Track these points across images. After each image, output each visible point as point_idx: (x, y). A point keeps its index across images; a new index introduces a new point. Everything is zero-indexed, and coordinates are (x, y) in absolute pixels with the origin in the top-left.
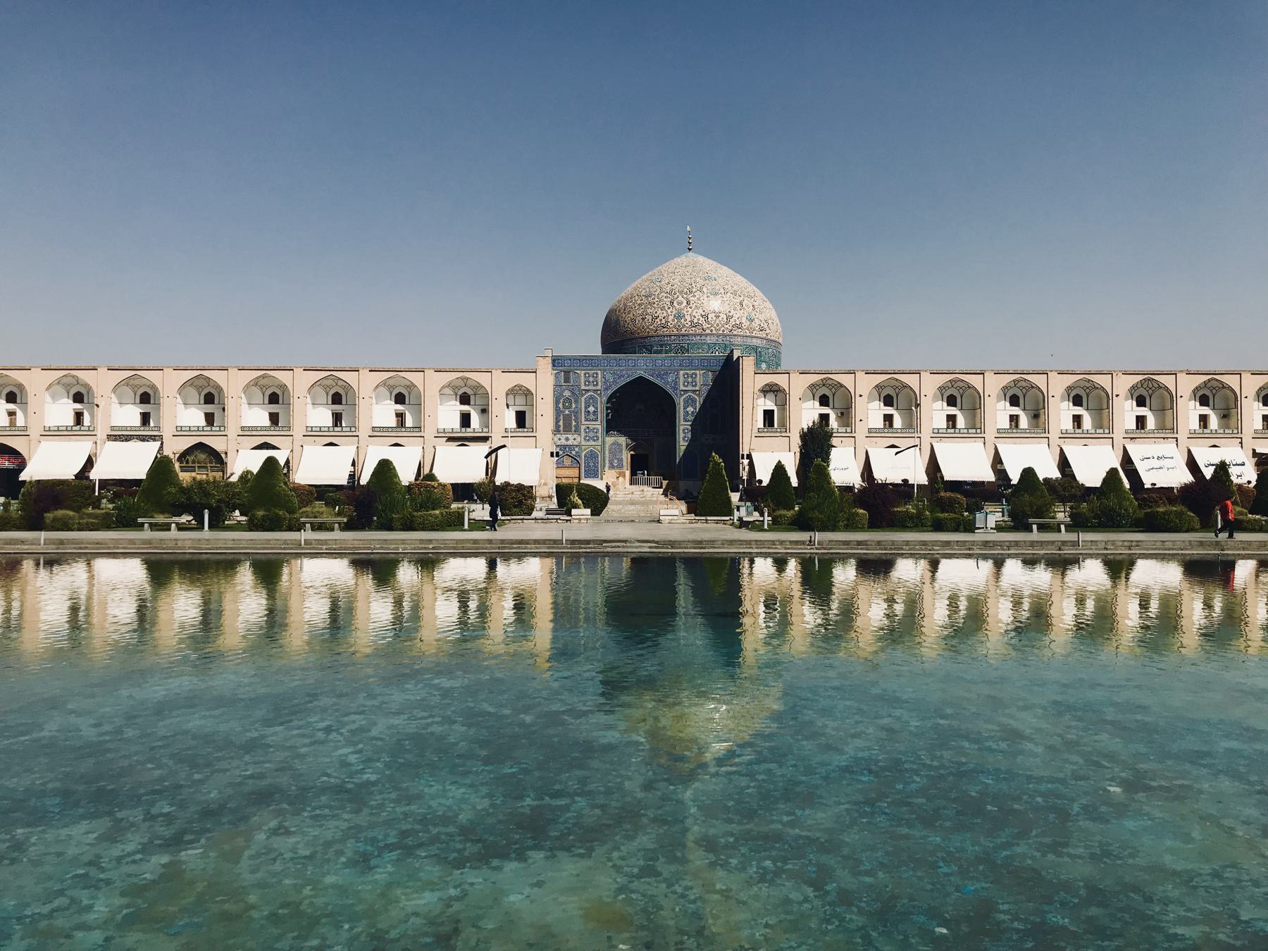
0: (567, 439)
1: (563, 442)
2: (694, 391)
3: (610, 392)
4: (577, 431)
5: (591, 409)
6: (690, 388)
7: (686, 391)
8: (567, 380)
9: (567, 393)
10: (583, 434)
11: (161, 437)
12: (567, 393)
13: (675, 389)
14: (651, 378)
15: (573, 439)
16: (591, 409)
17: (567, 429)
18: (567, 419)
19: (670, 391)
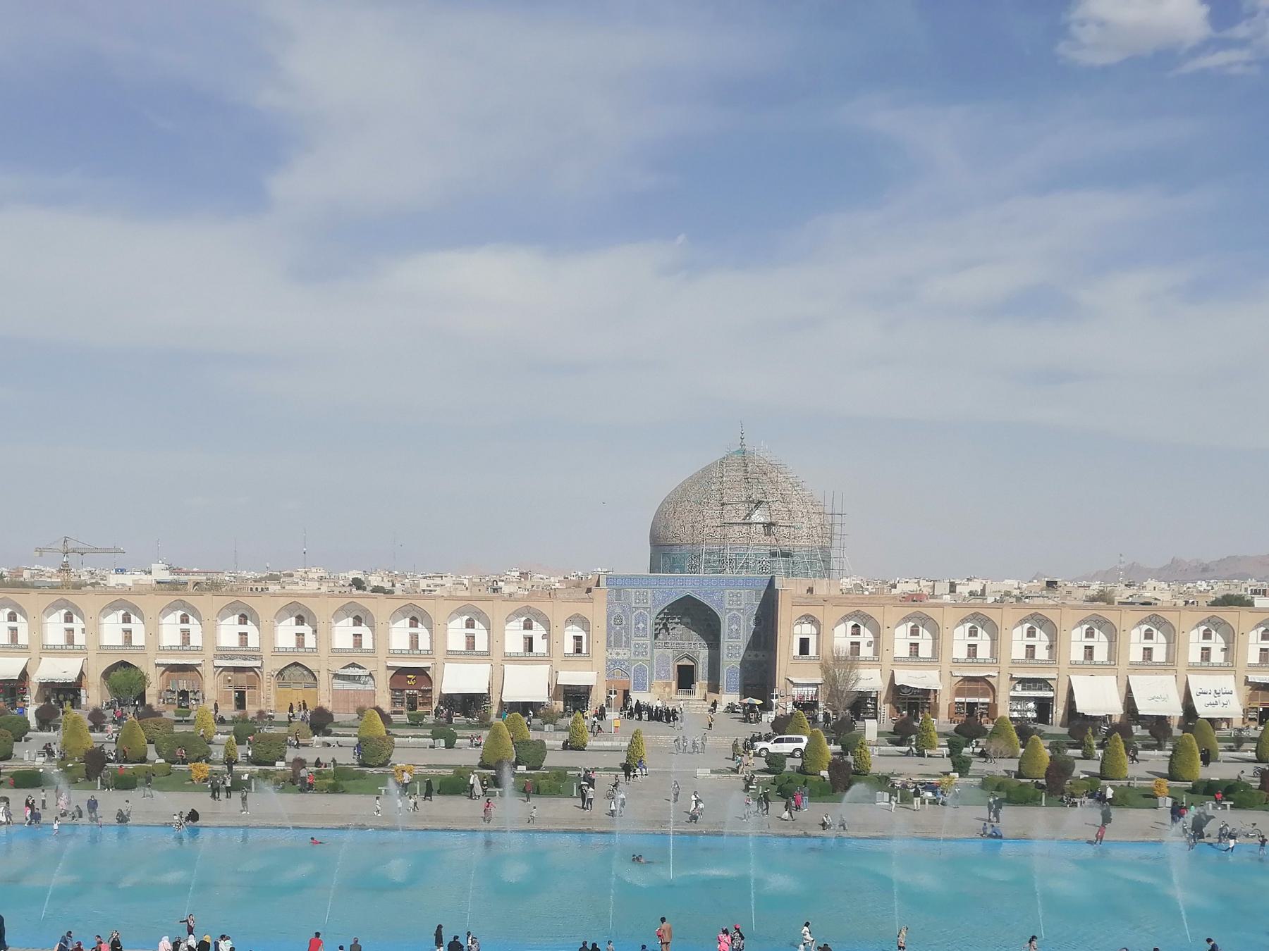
0: (618, 654)
1: (614, 656)
2: (738, 610)
3: (659, 610)
4: (627, 646)
5: (641, 625)
8: (618, 597)
9: (618, 611)
10: (633, 649)
12: (618, 611)
14: (698, 597)
15: (623, 654)
16: (641, 625)
17: (618, 644)
18: (618, 634)
19: (716, 610)
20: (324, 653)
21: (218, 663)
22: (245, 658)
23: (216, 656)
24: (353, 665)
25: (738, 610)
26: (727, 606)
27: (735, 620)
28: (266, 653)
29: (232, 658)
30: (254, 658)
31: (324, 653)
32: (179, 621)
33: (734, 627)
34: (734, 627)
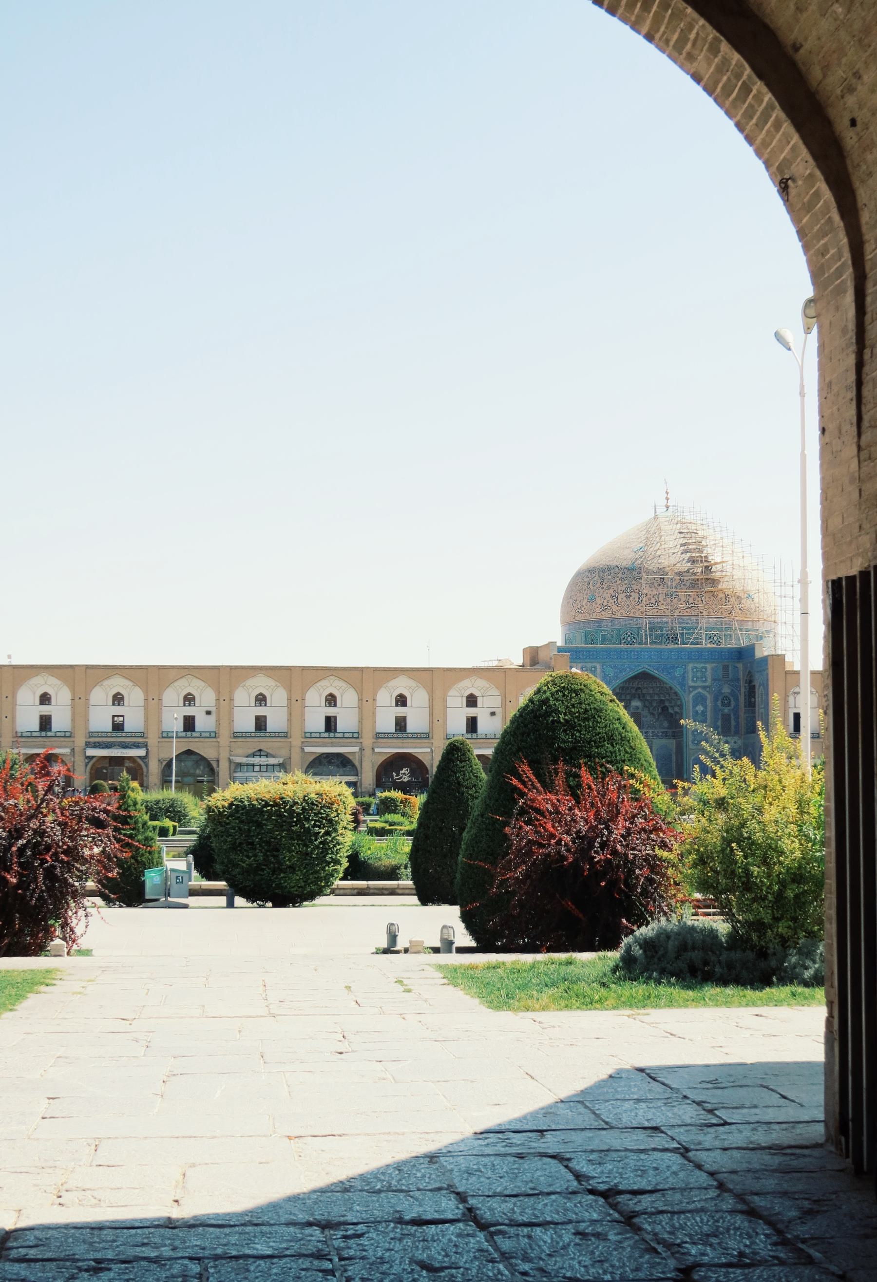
2: (704, 688)
6: (699, 684)
7: (695, 688)
11: (145, 746)
13: (682, 685)
14: (656, 673)
19: (678, 689)
20: (224, 739)
21: (90, 752)
22: (125, 746)
23: (88, 745)
24: (259, 753)
25: (704, 688)
26: (691, 684)
27: (700, 699)
28: (152, 740)
29: (108, 746)
30: (137, 746)
31: (224, 739)
32: (38, 702)
33: (700, 708)
34: (700, 708)
